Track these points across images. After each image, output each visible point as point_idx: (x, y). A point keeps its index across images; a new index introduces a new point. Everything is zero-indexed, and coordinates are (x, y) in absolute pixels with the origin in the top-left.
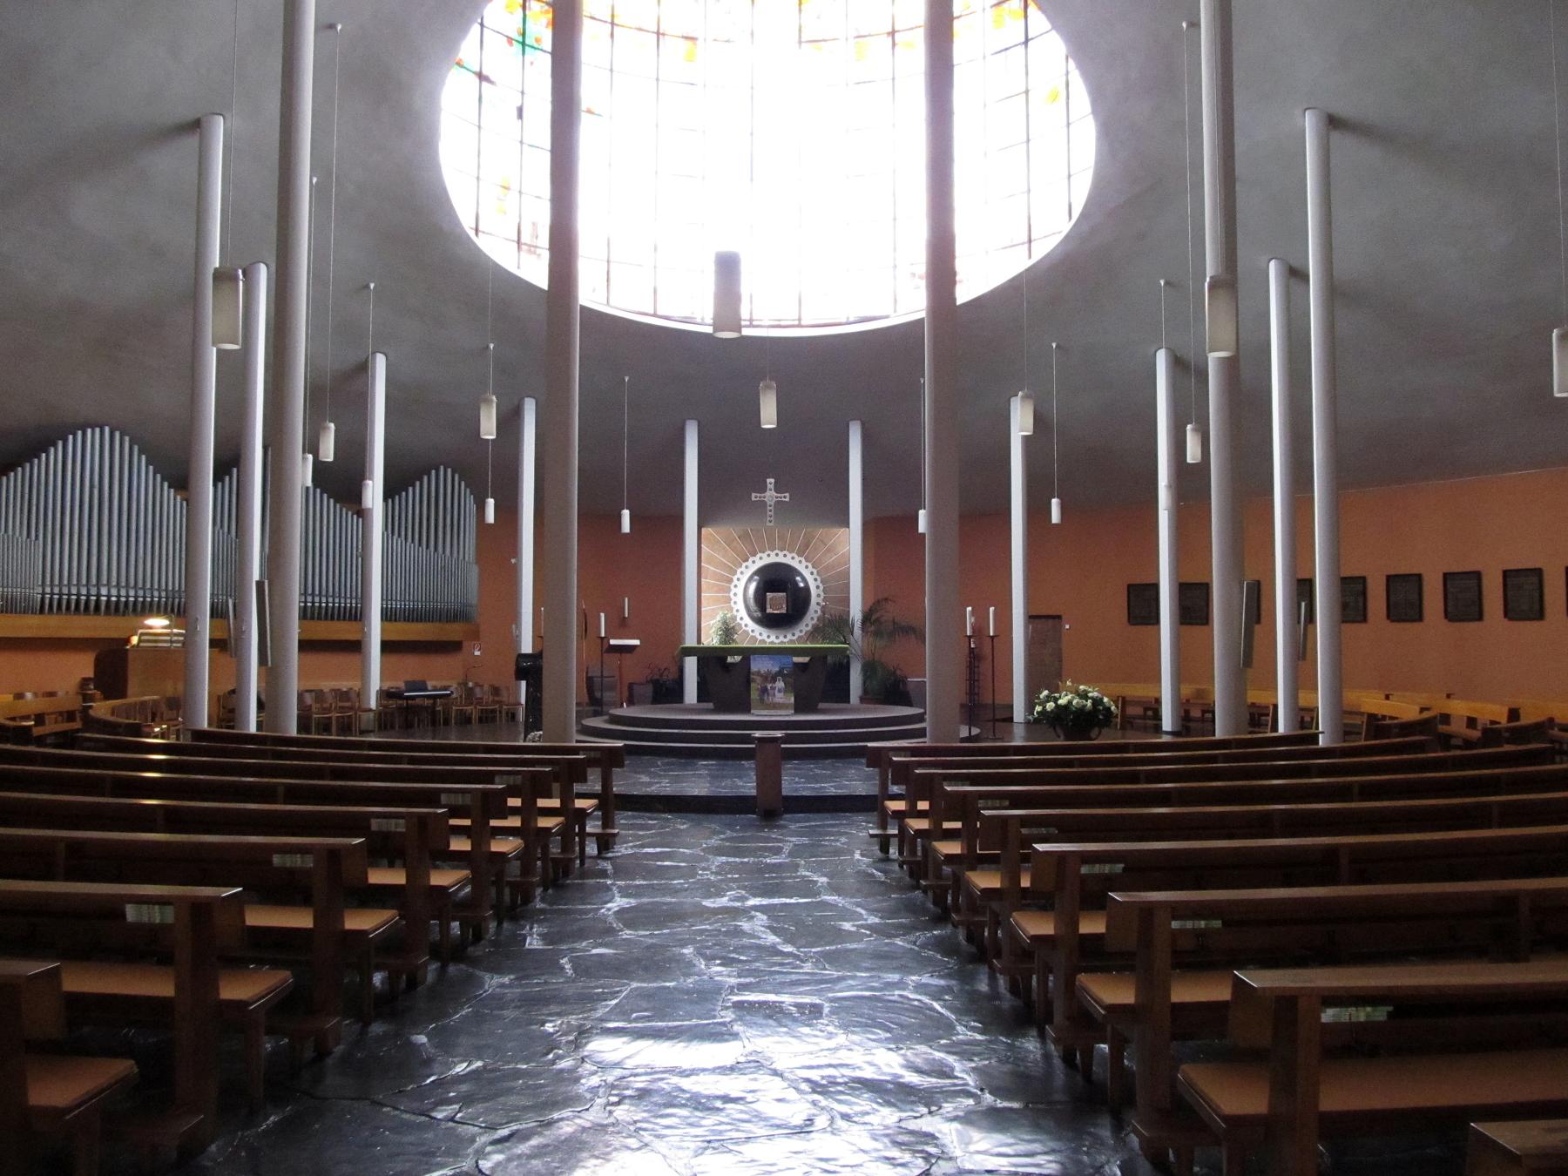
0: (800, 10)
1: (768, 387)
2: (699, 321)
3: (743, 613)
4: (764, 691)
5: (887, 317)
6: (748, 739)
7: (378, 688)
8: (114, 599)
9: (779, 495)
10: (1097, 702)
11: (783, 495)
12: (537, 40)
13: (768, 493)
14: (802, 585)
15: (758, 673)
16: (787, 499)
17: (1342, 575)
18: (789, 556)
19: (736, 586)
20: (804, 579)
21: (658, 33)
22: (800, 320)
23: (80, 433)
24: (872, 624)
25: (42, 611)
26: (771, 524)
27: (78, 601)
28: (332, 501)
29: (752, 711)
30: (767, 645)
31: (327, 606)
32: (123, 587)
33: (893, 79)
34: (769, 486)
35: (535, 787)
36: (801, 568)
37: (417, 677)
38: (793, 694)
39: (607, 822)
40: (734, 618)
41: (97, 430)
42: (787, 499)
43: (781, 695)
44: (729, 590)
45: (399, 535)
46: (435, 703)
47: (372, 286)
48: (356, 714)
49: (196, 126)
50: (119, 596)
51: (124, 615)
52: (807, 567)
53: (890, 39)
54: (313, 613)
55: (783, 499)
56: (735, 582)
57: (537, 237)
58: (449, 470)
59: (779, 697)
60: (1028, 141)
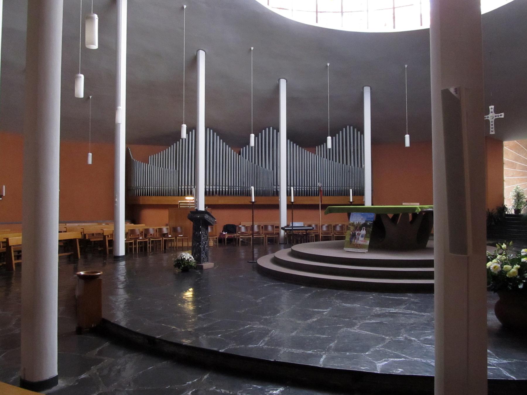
4: (353, 236)
9: (497, 115)
16: (503, 117)
28: (298, 146)
31: (222, 190)
32: (211, 185)
34: (491, 110)
38: (369, 239)
43: (361, 239)
47: (252, 48)
55: (500, 117)
58: (352, 128)
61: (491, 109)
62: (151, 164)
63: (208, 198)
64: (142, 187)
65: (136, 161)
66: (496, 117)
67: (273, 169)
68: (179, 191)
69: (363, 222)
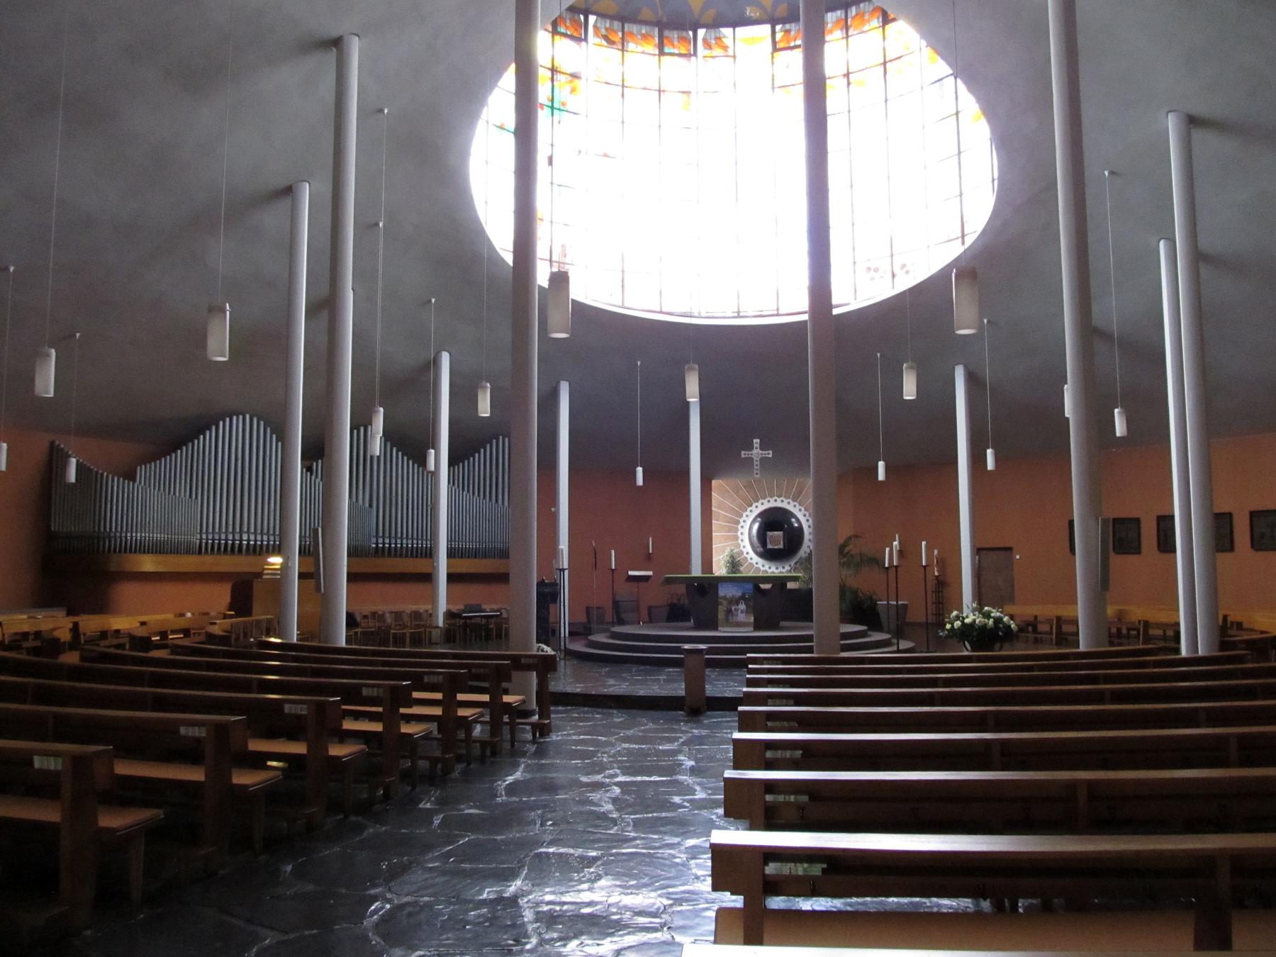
0: (773, 63)
1: (691, 369)
2: (696, 314)
3: (749, 548)
4: (729, 611)
5: (848, 304)
6: (678, 650)
7: (445, 610)
8: (252, 543)
9: (764, 452)
10: (998, 621)
11: (767, 452)
12: (563, 104)
13: (755, 451)
14: (796, 525)
15: (725, 598)
16: (770, 456)
17: (1217, 511)
18: (786, 501)
19: (742, 527)
20: (798, 520)
21: (660, 91)
22: (778, 310)
23: (228, 419)
24: (844, 556)
25: (200, 552)
26: (758, 476)
27: (226, 544)
29: (719, 629)
30: (769, 575)
33: (849, 111)
34: (755, 445)
35: (453, 685)
36: (795, 511)
37: (473, 602)
39: (544, 713)
40: (742, 552)
41: (241, 417)
42: (770, 456)
43: (743, 615)
44: (737, 530)
45: (468, 491)
46: (488, 623)
47: (433, 300)
48: (425, 630)
49: (288, 191)
50: (255, 541)
51: (260, 555)
52: (800, 510)
53: (846, 80)
54: (402, 552)
56: (742, 524)
57: (565, 256)
59: (741, 617)
60: (959, 153)
61: (756, 443)
62: (140, 482)
63: (452, 560)
64: (118, 535)
65: (105, 474)
66: (762, 454)
67: (371, 506)
68: (201, 543)
69: (739, 594)
